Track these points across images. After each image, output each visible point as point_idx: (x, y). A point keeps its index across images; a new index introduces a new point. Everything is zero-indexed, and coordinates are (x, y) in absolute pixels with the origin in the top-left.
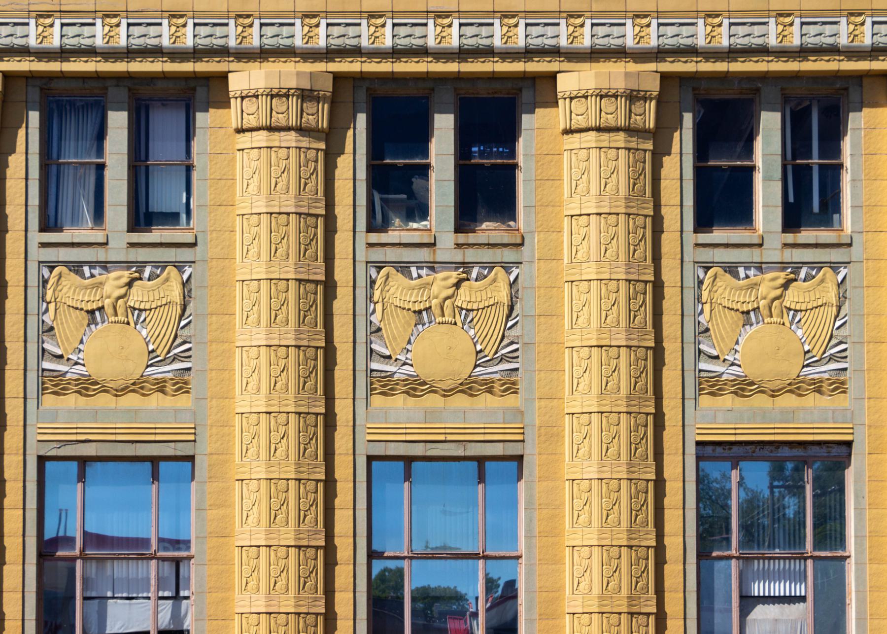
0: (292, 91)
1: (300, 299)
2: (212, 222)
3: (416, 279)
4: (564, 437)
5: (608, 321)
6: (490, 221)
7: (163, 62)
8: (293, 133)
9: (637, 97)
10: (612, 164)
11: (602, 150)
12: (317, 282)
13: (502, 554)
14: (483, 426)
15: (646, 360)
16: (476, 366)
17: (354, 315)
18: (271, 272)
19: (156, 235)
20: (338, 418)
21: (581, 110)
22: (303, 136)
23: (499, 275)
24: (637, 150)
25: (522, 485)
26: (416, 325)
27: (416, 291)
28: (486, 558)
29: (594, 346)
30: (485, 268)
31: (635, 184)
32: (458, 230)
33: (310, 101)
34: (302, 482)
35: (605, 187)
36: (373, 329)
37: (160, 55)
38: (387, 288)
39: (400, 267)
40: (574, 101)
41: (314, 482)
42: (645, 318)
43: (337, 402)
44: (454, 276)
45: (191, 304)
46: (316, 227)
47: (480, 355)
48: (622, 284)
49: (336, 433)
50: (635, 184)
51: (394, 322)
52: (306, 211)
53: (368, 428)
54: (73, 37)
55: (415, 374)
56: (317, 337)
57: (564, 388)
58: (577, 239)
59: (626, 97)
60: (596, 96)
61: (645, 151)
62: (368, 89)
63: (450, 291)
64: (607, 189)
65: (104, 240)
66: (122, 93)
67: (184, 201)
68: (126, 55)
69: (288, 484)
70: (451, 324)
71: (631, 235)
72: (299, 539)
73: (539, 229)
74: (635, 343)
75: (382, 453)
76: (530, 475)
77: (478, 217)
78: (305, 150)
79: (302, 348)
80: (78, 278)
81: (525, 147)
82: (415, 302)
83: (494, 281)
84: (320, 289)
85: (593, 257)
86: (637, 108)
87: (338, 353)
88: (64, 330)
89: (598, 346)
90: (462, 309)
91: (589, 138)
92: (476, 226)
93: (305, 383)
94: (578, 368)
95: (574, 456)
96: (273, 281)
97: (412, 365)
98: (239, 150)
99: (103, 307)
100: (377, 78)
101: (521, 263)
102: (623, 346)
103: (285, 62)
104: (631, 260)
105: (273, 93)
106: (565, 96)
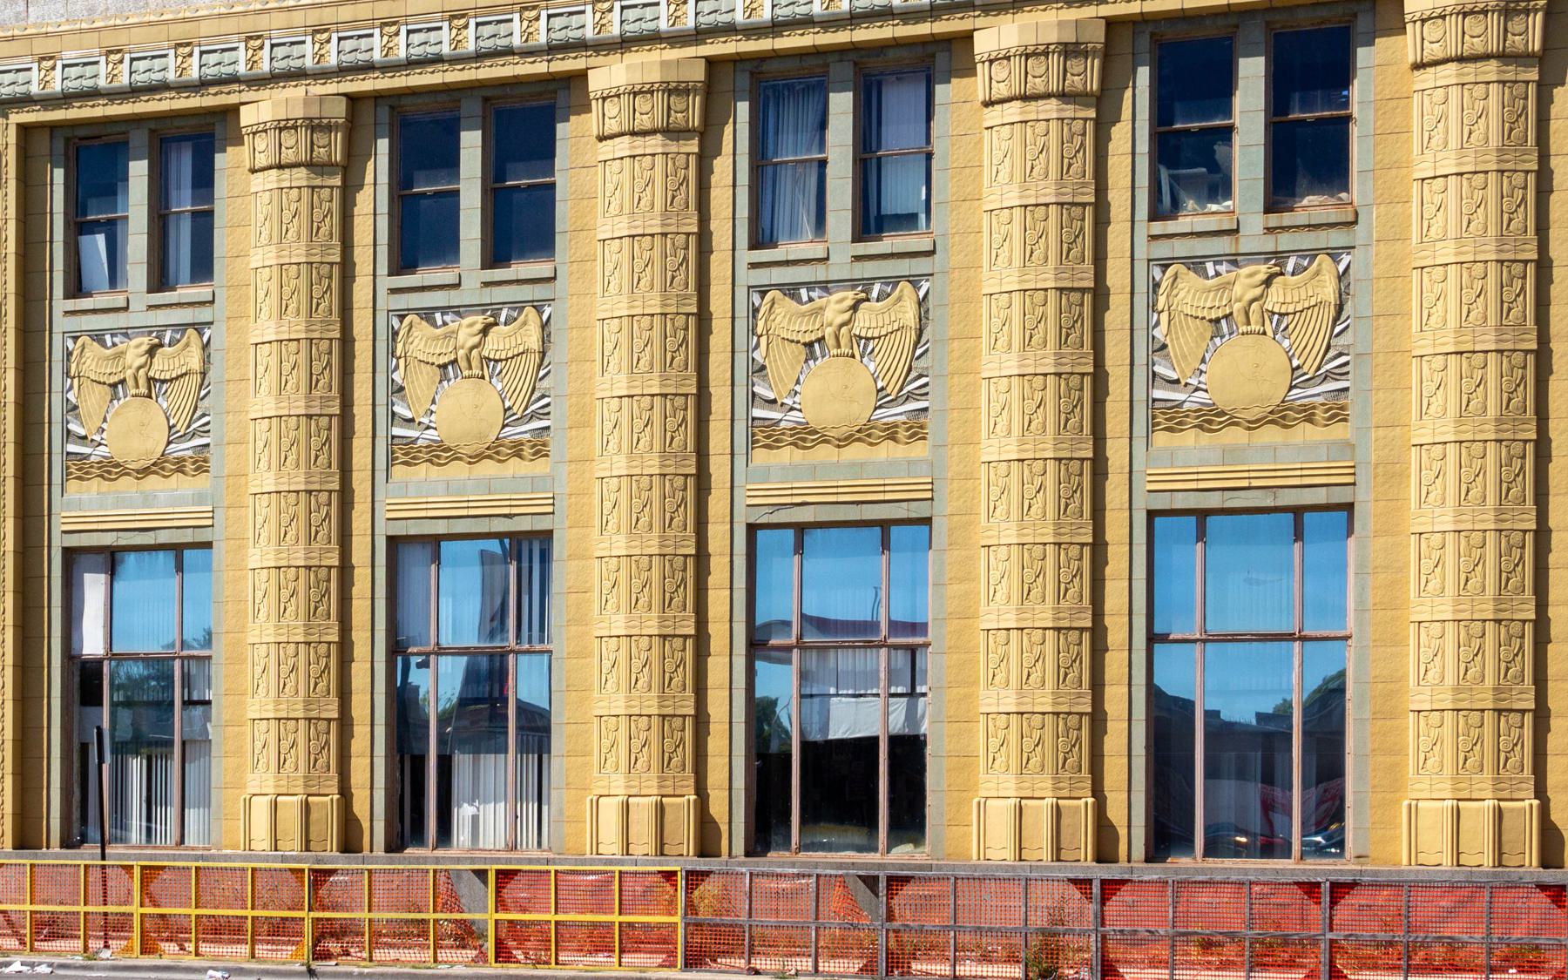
0: (1052, 47)
1: (1061, 314)
2: (954, 223)
3: (1212, 277)
4: (1409, 476)
5: (1470, 318)
6: (1314, 195)
7: (893, 25)
8: (1054, 101)
9: (1516, 10)
10: (1480, 105)
11: (1466, 87)
12: (1083, 290)
13: (1325, 633)
14: (1299, 466)
15: (1525, 367)
16: (1291, 388)
17: (1132, 330)
18: (1025, 281)
19: (888, 244)
20: (1110, 463)
21: (1437, 35)
22: (1067, 104)
23: (1324, 266)
24: (1516, 82)
25: (1351, 542)
26: (1212, 338)
27: (1212, 294)
28: (1303, 639)
29: (1451, 353)
30: (1304, 257)
31: (1511, 130)
32: (1269, 209)
33: (1076, 57)
34: (1063, 546)
35: (1469, 137)
36: (1157, 346)
37: (891, 17)
38: (1175, 292)
39: (1193, 263)
40: (1426, 25)
41: (1078, 547)
42: (1525, 311)
43: (1109, 443)
44: (1263, 270)
45: (929, 328)
46: (1083, 220)
47: (1297, 373)
48: (1492, 267)
49: (1107, 483)
50: (1511, 130)
51: (1184, 335)
52: (1071, 200)
53: (1149, 475)
54: (786, 6)
55: (1210, 402)
56: (1083, 360)
57: (1410, 412)
58: (1429, 210)
59: (1500, 11)
60: (1458, 14)
61: (1527, 82)
62: (1152, 35)
63: (1258, 291)
64: (1472, 139)
65: (822, 255)
66: (845, 70)
67: (924, 197)
68: (849, 22)
69: (1045, 550)
70: (1258, 333)
71: (1504, 200)
72: (1059, 619)
73: (1379, 201)
74: (1509, 346)
75: (1167, 507)
76: (1363, 529)
77: (1298, 190)
78: (1070, 121)
79: (1063, 376)
80: (794, 304)
81: (1361, 92)
82: (1211, 308)
83: (1317, 273)
84: (1088, 298)
85: (1452, 233)
86: (1516, 24)
87: (1111, 380)
88: (777, 368)
89: (1456, 353)
90: (1274, 313)
91: (1448, 72)
92: (1295, 202)
93: (1067, 420)
94: (1429, 383)
95: (1423, 501)
96: (1027, 293)
97: (1206, 391)
98: (987, 128)
99: (823, 338)
100: (1164, 19)
101: (1354, 247)
102: (1492, 351)
103: (1045, 10)
104: (1504, 233)
105: (1028, 51)
106: (1415, 19)
